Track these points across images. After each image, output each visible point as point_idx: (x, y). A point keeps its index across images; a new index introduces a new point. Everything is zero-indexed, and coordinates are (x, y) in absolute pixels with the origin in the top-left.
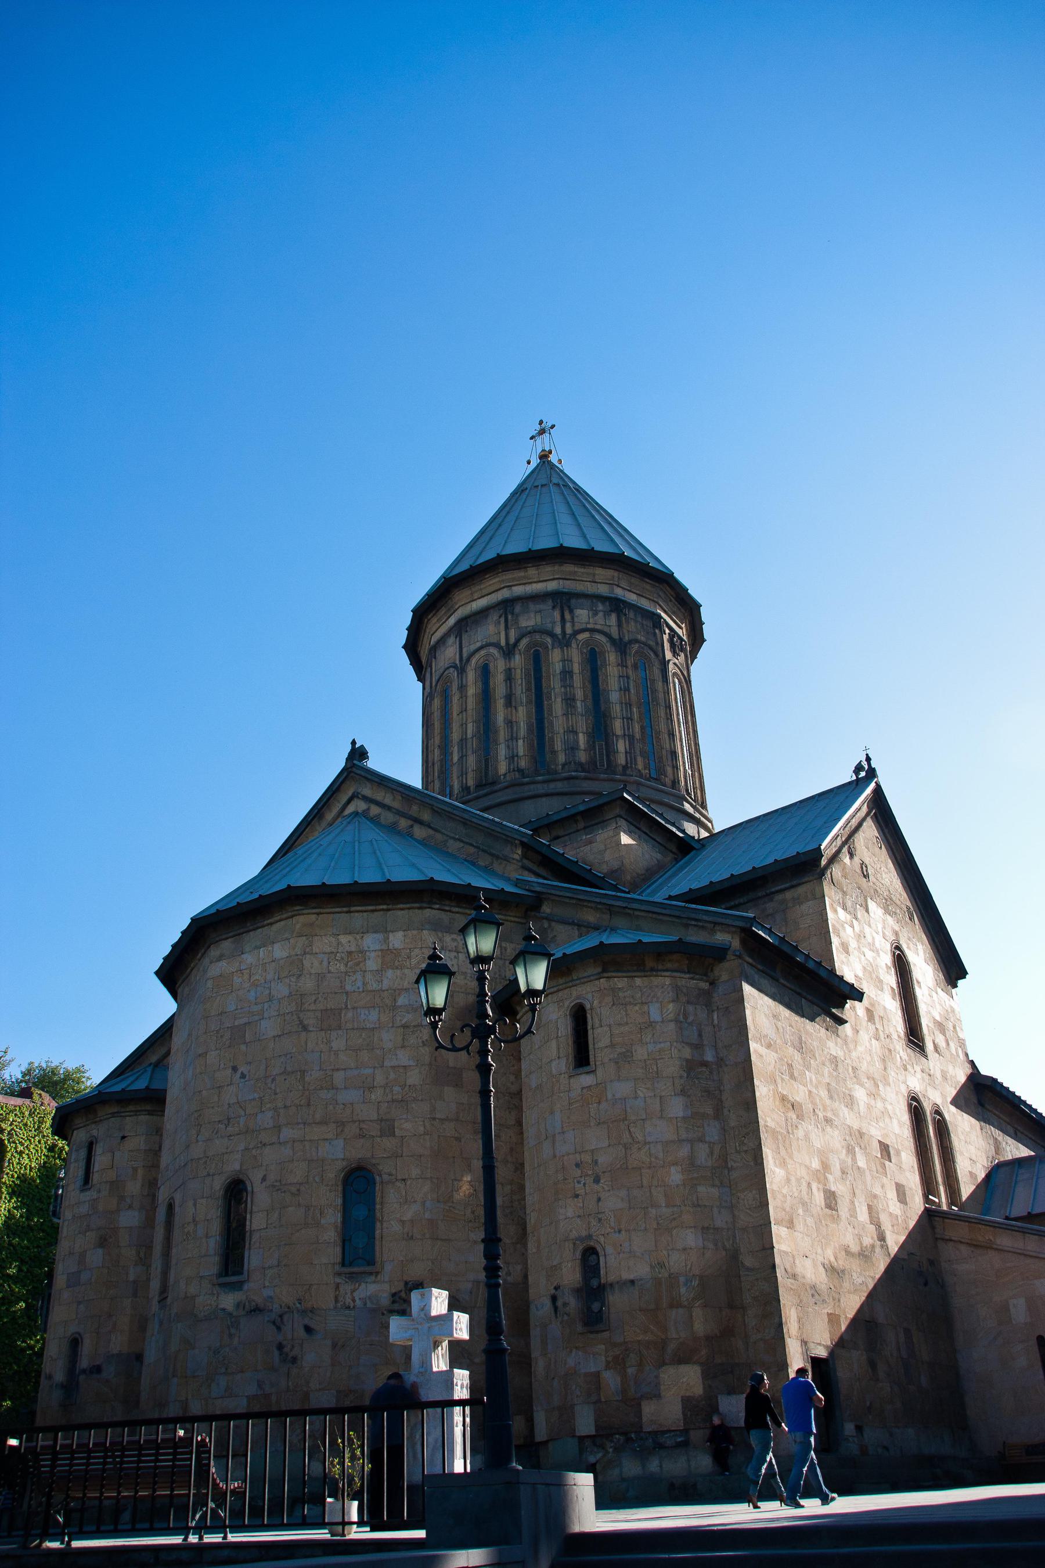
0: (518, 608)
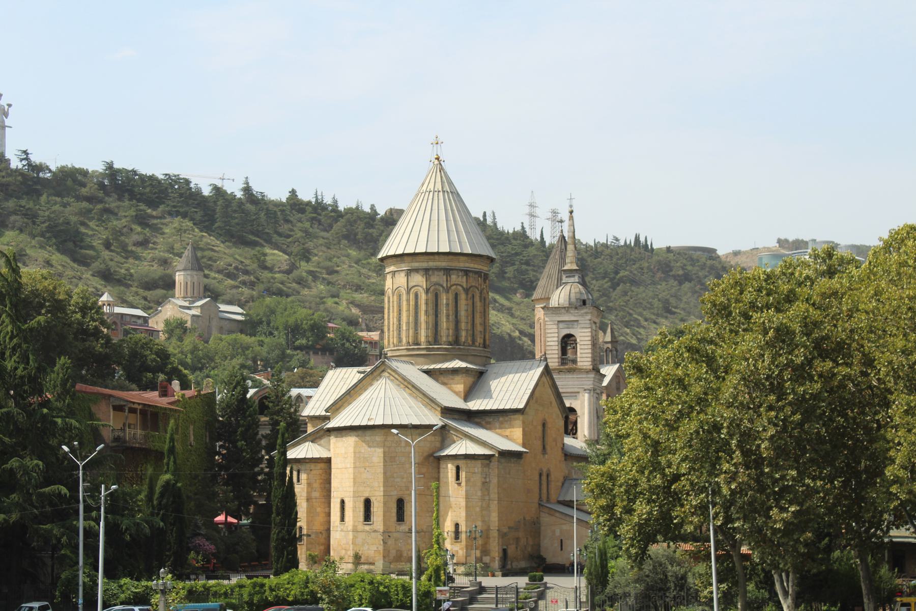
0: (430, 272)
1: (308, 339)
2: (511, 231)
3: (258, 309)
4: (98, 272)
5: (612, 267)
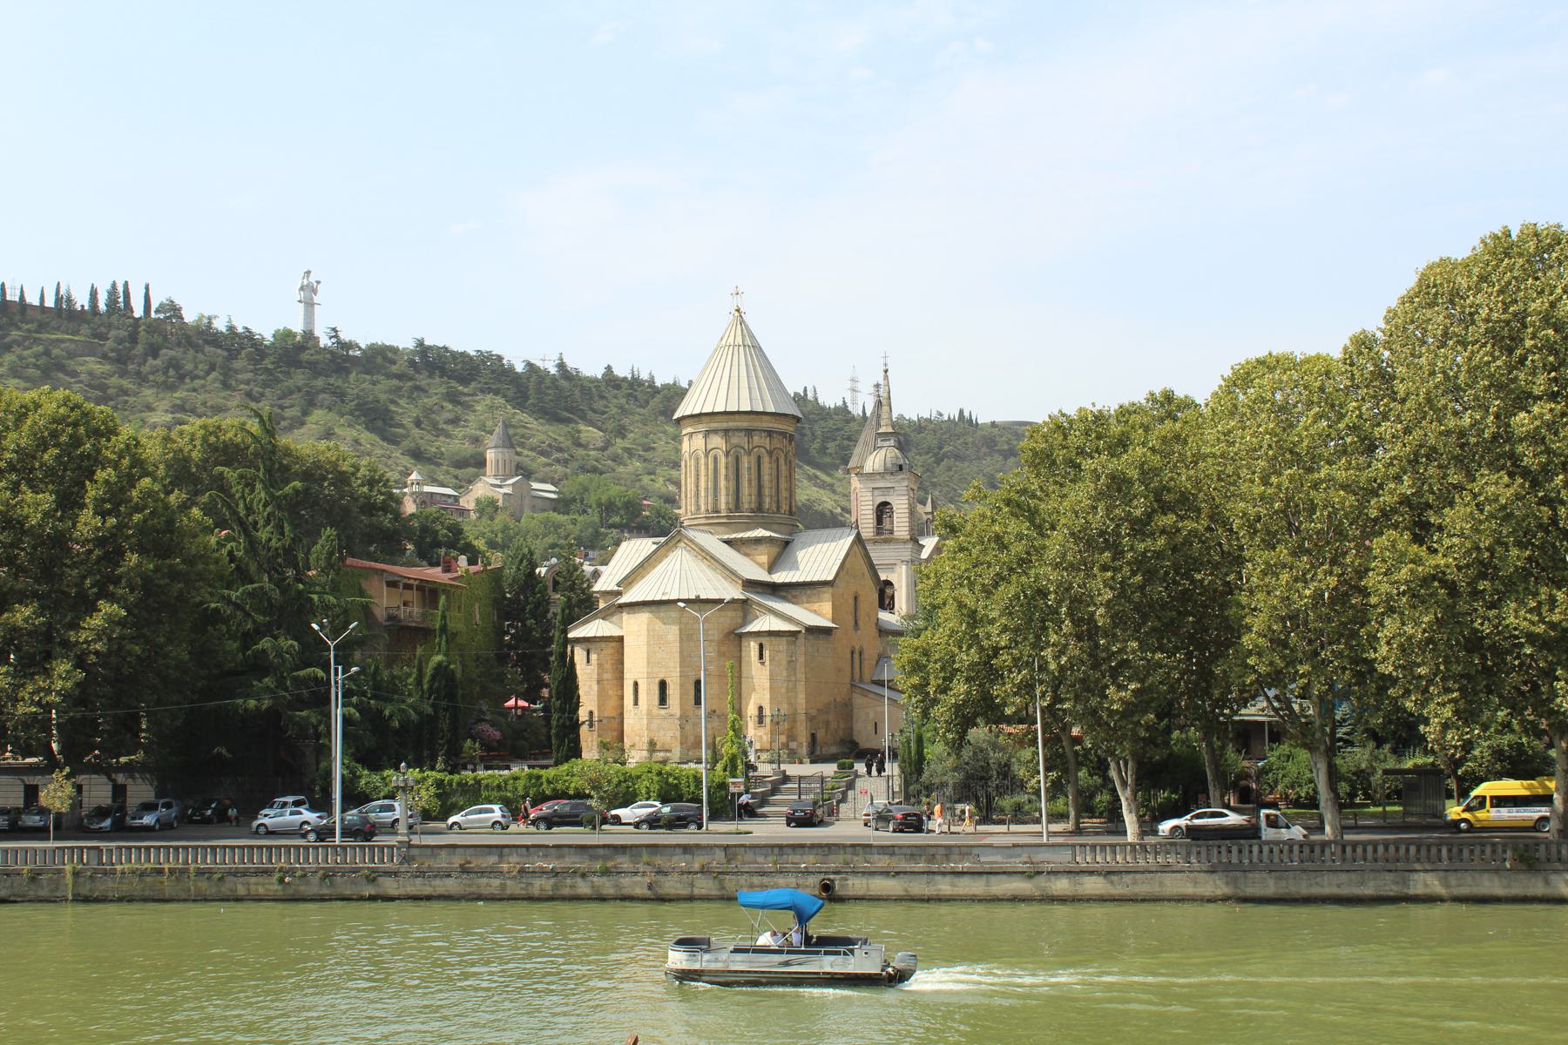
1: (621, 516)
2: (832, 407)
3: (570, 487)
4: (408, 451)
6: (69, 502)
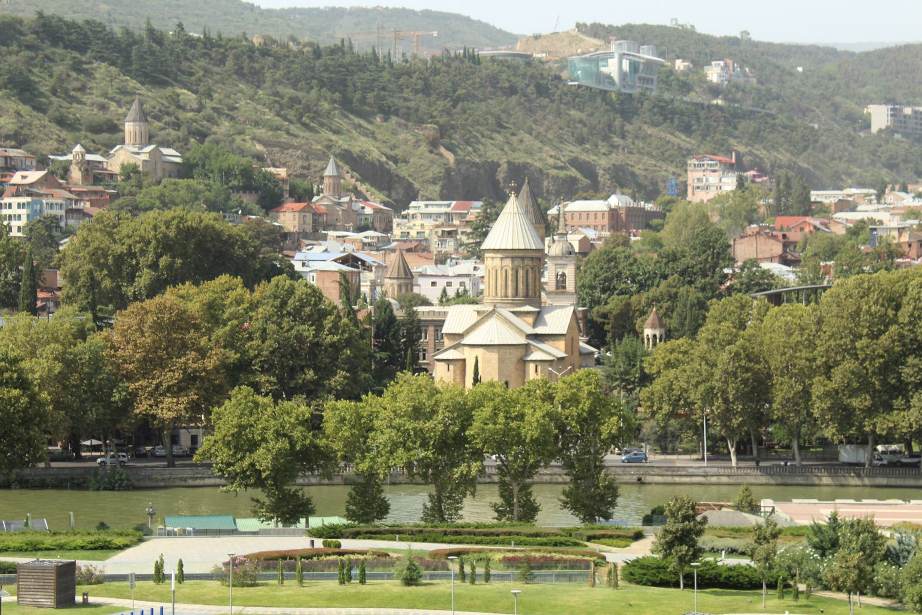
1: (239, 181)
5: (450, 84)
6: (320, 328)
